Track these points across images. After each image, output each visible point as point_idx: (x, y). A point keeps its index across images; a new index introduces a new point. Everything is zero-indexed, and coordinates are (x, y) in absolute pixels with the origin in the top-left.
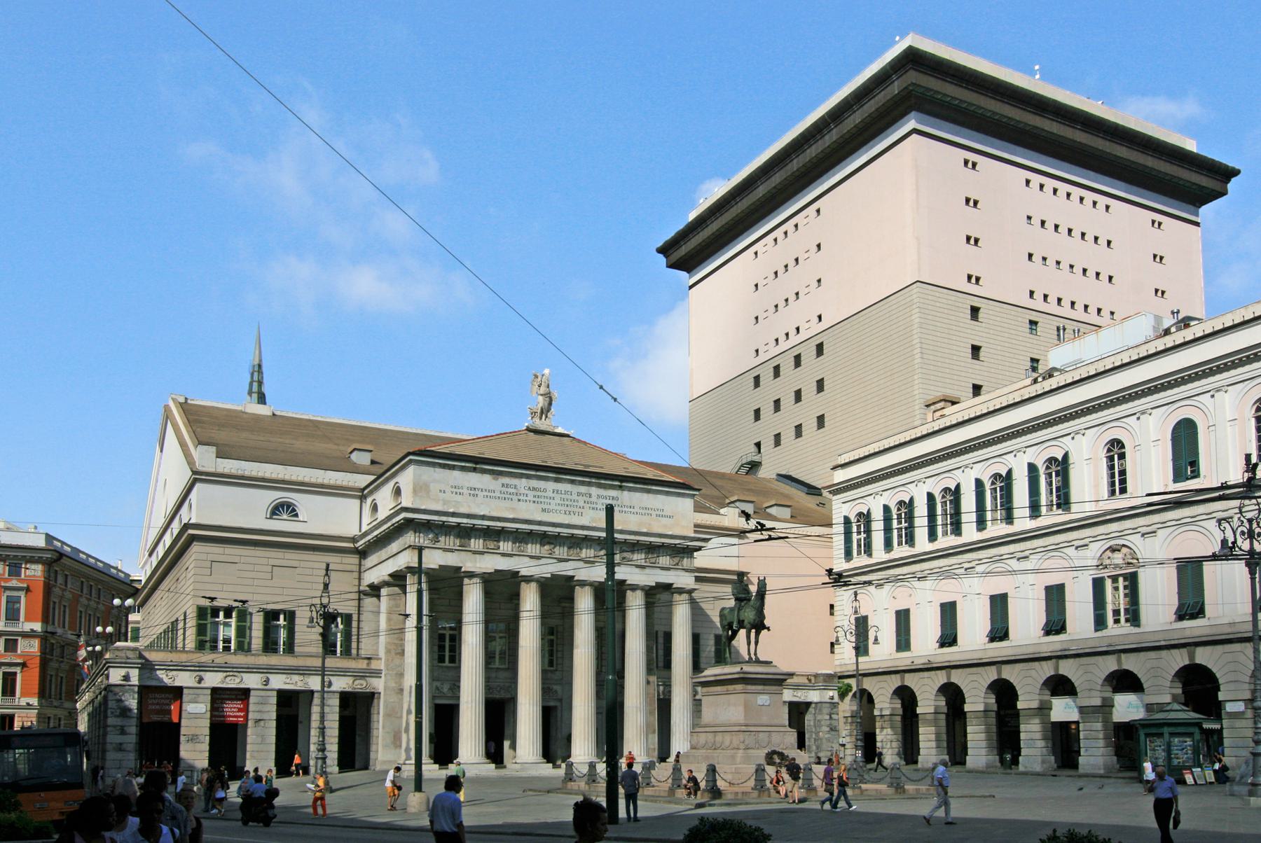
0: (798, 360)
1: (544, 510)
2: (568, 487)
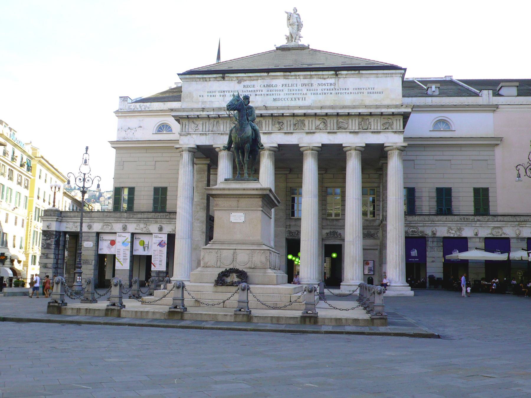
1: (275, 100)
2: (295, 81)
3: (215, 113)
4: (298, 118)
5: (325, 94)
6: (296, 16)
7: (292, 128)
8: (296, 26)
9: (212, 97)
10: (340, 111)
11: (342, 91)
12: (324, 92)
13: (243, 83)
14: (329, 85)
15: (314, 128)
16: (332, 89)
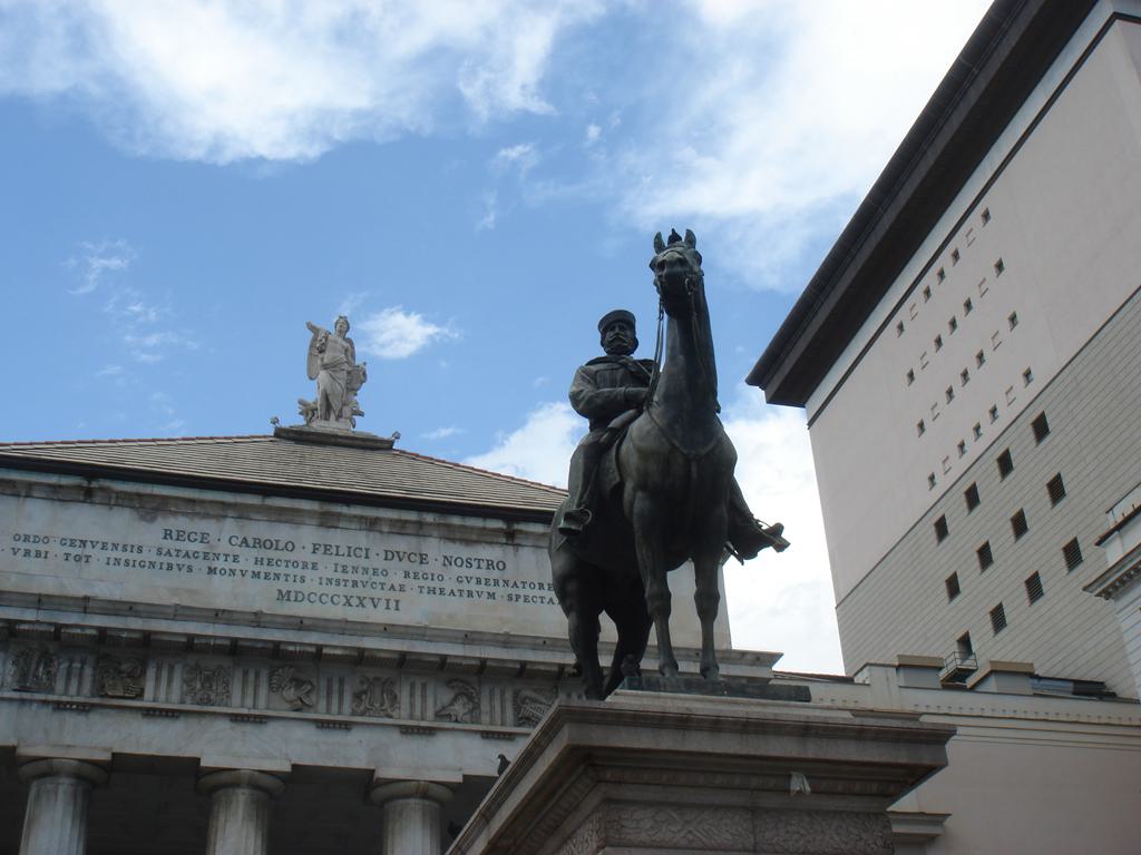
0: (1005, 464)
2: (361, 539)
3: (43, 616)
4: (371, 673)
5: (470, 594)
6: (346, 345)
7: (347, 707)
8: (344, 375)
9: (33, 559)
10: (530, 656)
11: (531, 593)
12: (465, 586)
13: (163, 523)
14: (484, 565)
15: (430, 714)
16: (496, 583)
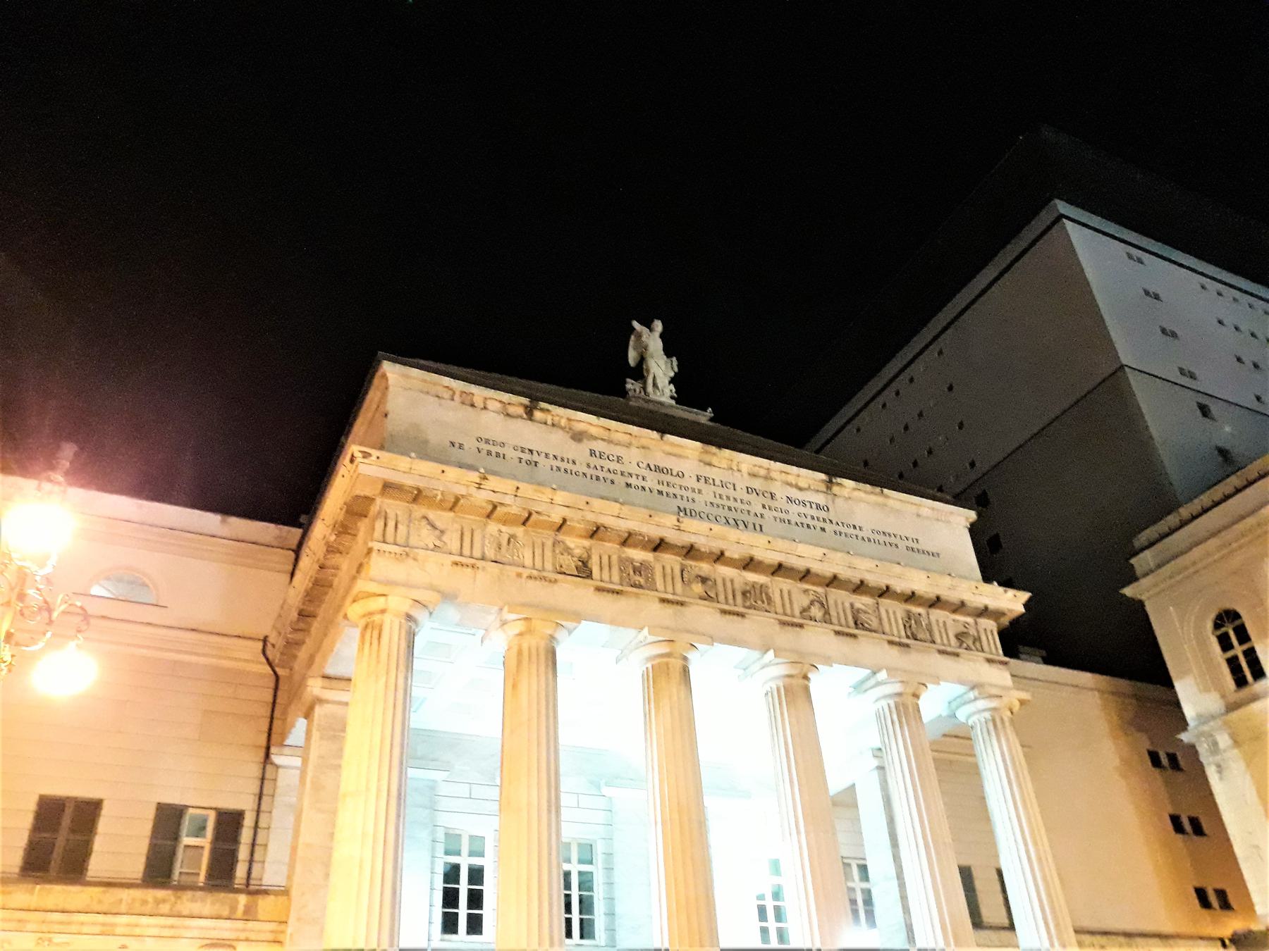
4: (752, 577)
